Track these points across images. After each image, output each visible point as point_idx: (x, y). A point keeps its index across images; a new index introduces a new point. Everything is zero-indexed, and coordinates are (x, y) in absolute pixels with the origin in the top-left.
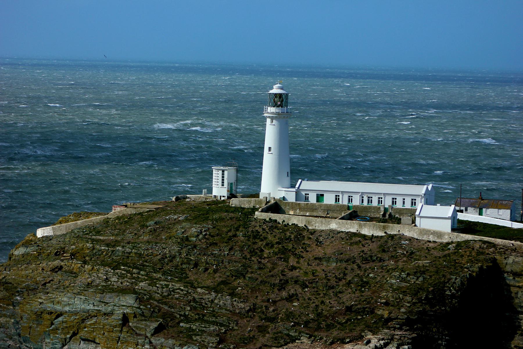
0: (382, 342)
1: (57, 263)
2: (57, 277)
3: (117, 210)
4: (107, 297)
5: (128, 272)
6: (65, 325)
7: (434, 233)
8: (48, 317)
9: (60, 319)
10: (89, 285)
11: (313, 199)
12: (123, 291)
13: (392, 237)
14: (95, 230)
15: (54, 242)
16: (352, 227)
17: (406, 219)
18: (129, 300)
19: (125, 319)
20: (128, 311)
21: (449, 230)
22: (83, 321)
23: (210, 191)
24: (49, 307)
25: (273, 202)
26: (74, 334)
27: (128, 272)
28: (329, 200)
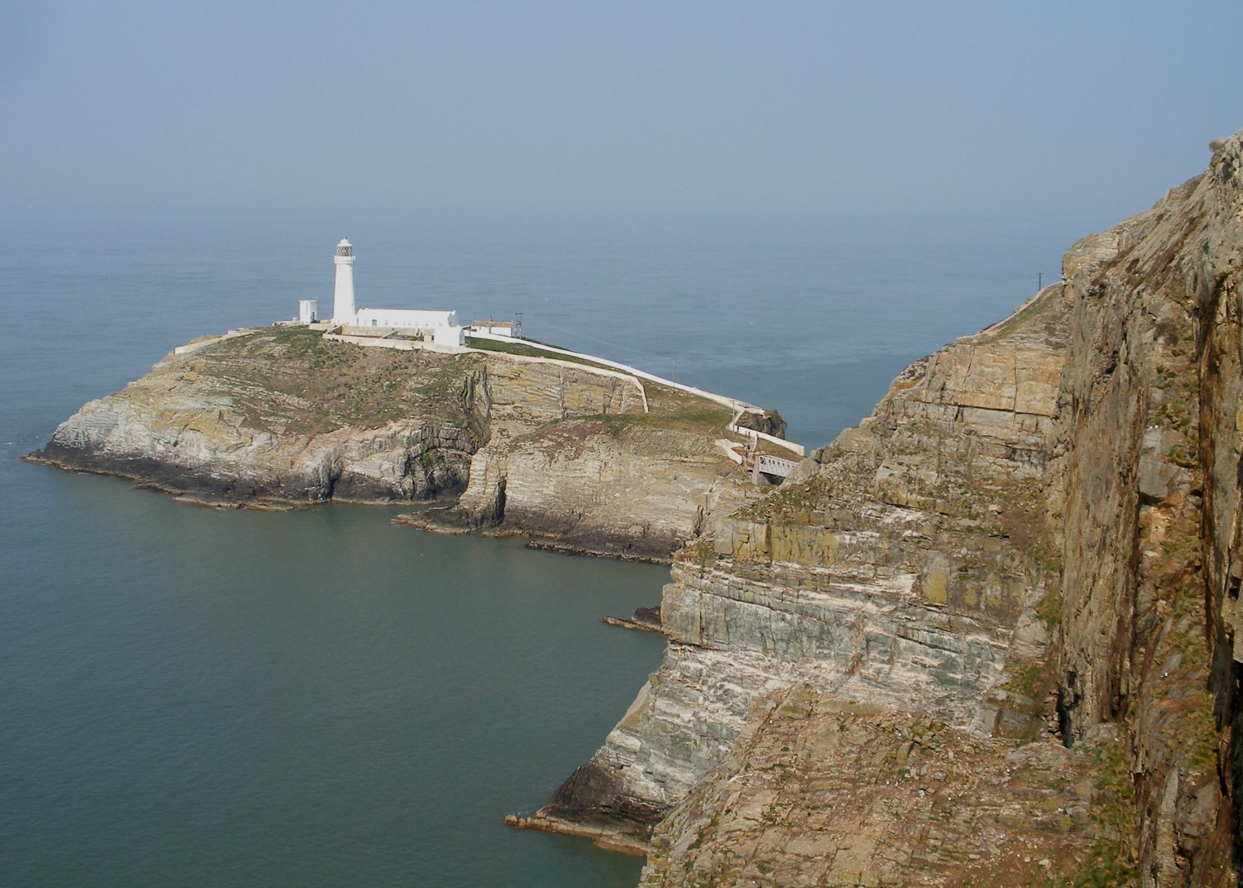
0: (400, 428)
1: (181, 374)
2: (180, 384)
3: (232, 334)
4: (211, 399)
5: (228, 379)
6: (179, 420)
7: (446, 347)
8: (169, 414)
9: (177, 415)
10: (199, 390)
11: (370, 324)
12: (222, 394)
13: (417, 350)
14: (209, 348)
15: (182, 358)
16: (390, 344)
17: (427, 338)
18: (227, 400)
19: (221, 415)
20: (223, 408)
21: (458, 346)
22: (192, 416)
23: (299, 319)
24: (172, 406)
25: (339, 326)
26: (186, 426)
27: (228, 379)
28: (380, 324)
